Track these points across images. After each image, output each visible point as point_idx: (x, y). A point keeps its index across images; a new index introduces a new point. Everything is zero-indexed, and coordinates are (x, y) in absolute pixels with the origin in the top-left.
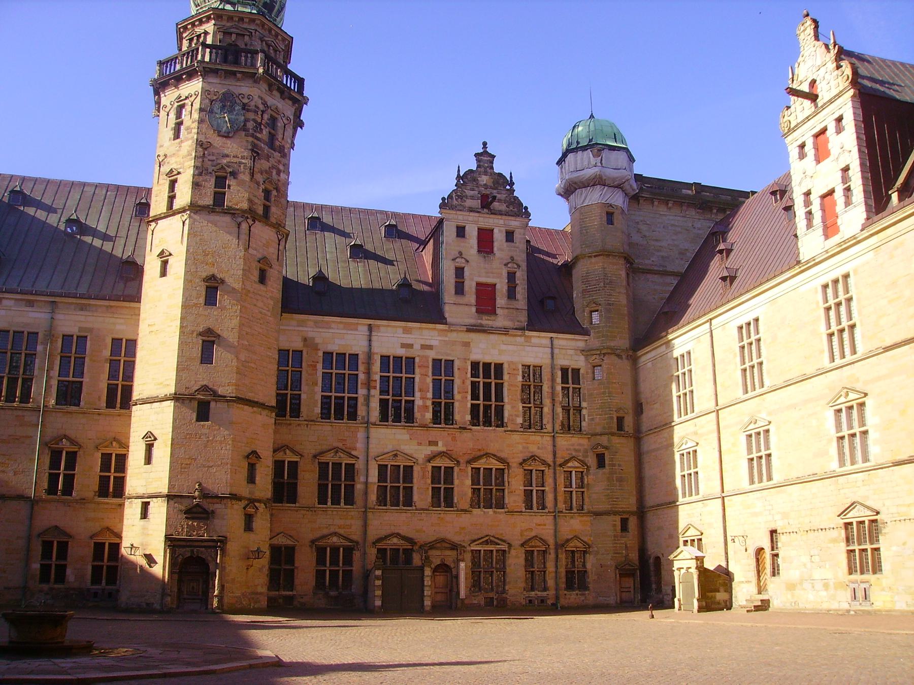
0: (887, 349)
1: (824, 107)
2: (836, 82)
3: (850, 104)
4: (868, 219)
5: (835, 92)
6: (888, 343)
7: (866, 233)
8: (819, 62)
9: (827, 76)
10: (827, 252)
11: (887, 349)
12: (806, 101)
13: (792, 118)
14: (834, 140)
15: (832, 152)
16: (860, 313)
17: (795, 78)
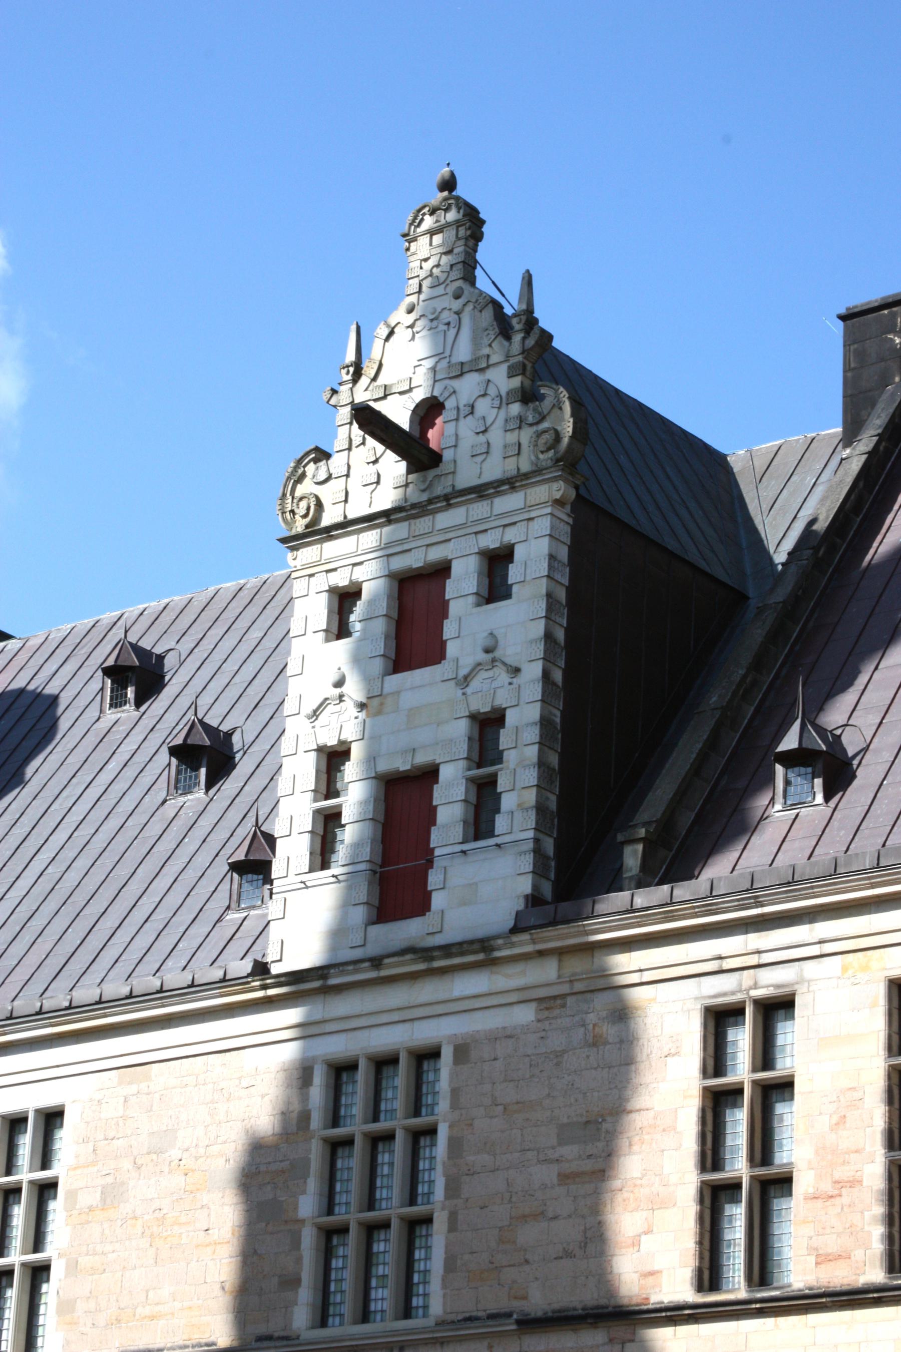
0: (530, 1324)
1: (449, 500)
2: (512, 437)
3: (543, 525)
4: (534, 900)
5: (494, 469)
6: (538, 1302)
7: (524, 944)
8: (463, 352)
9: (483, 407)
10: (376, 962)
11: (530, 1324)
12: (390, 457)
13: (329, 494)
14: (466, 623)
15: (451, 649)
16: (453, 1189)
17: (369, 370)
